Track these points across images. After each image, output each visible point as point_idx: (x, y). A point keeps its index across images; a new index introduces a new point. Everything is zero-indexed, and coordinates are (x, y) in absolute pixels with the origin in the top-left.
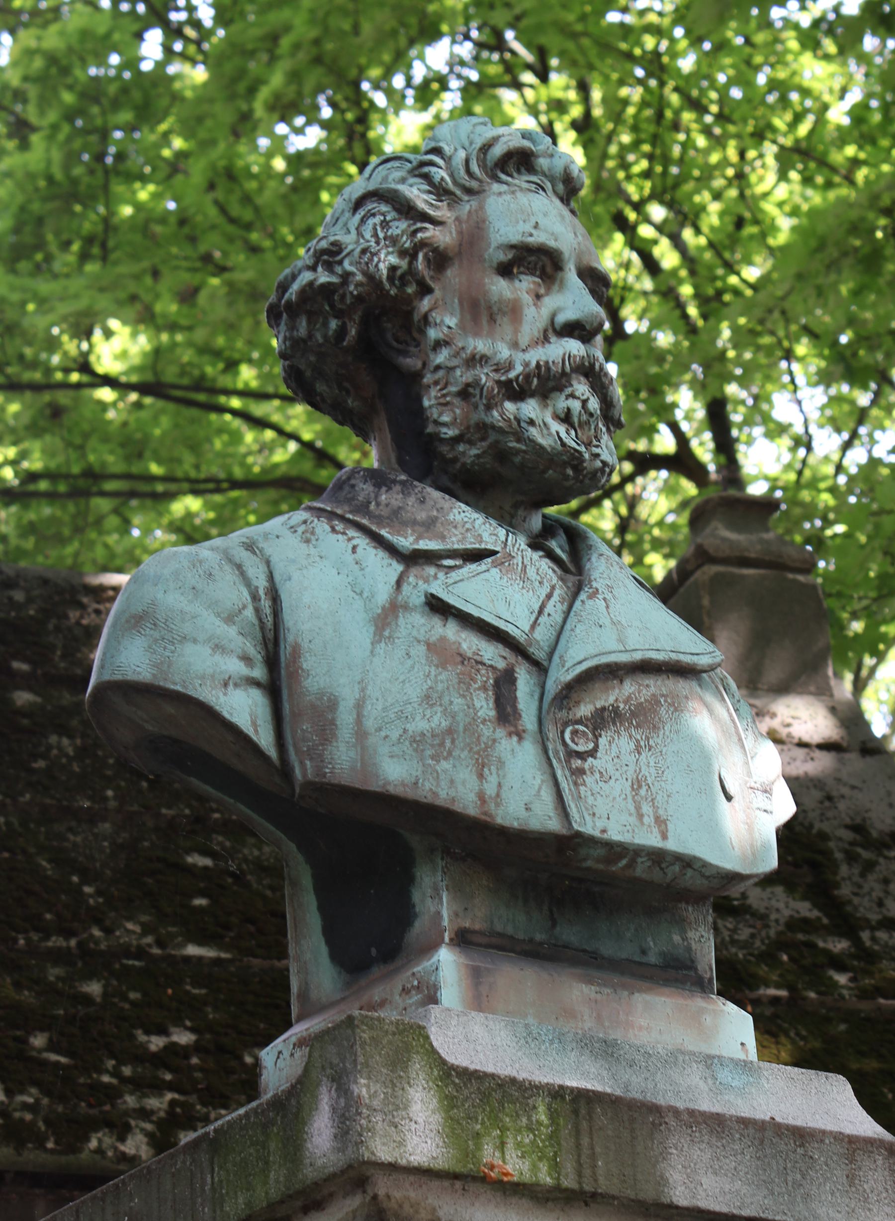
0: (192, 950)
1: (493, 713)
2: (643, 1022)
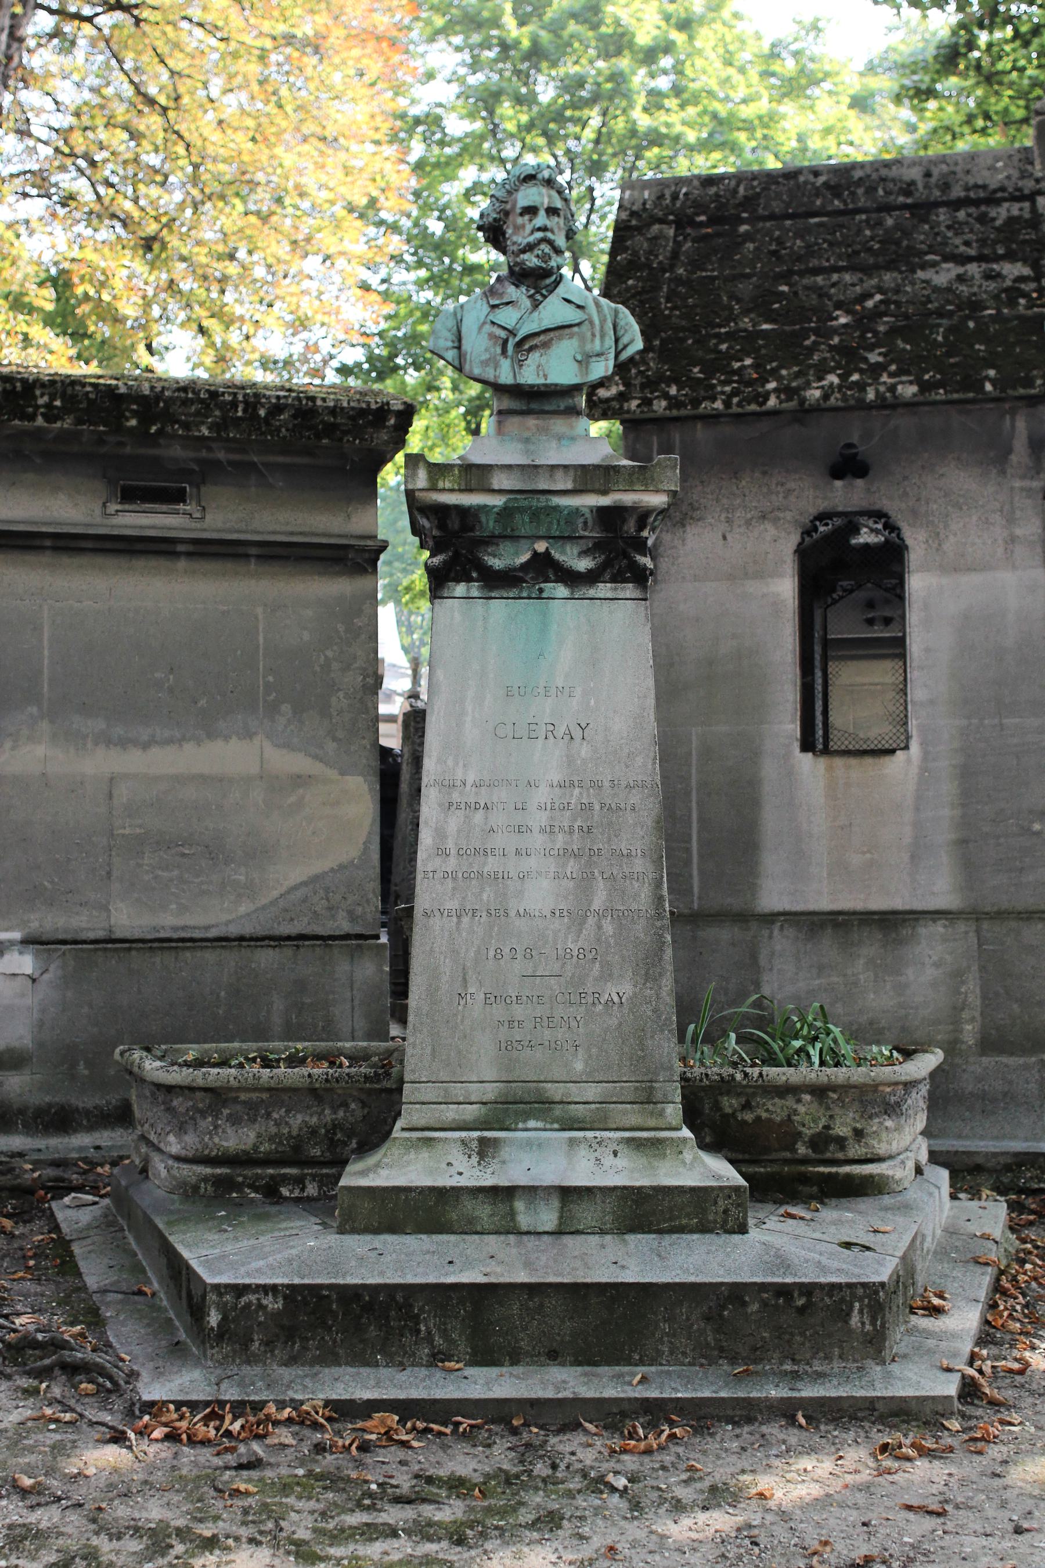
0: (765, 327)
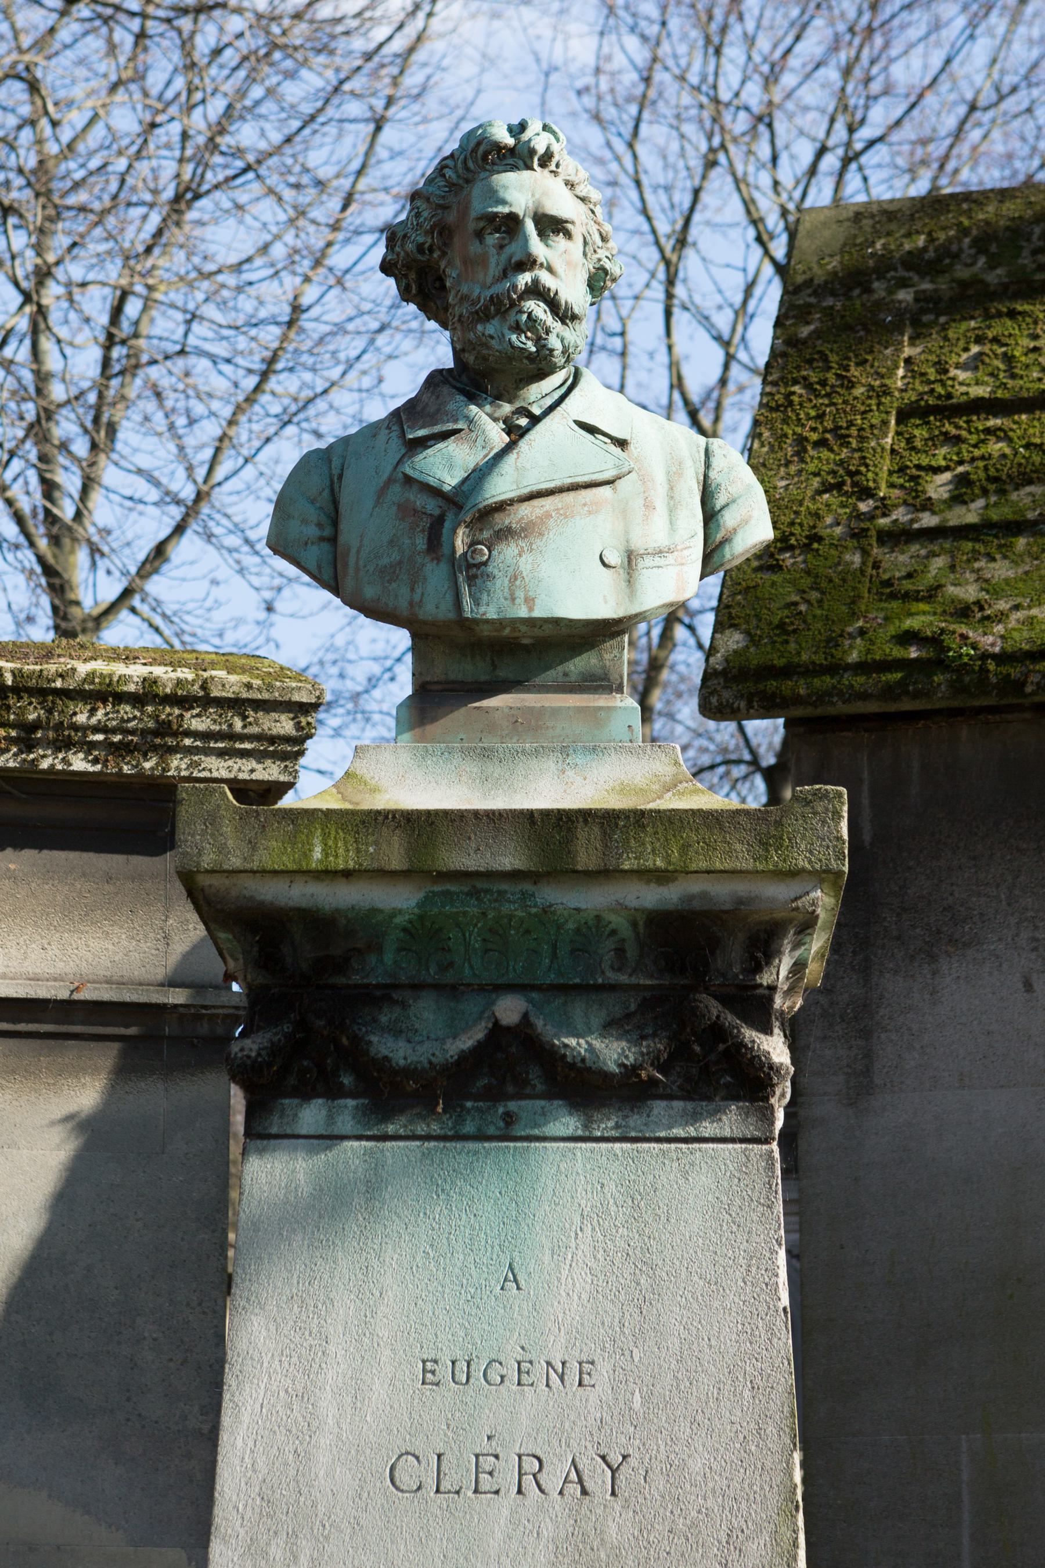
1: (425, 547)
2: (549, 724)
